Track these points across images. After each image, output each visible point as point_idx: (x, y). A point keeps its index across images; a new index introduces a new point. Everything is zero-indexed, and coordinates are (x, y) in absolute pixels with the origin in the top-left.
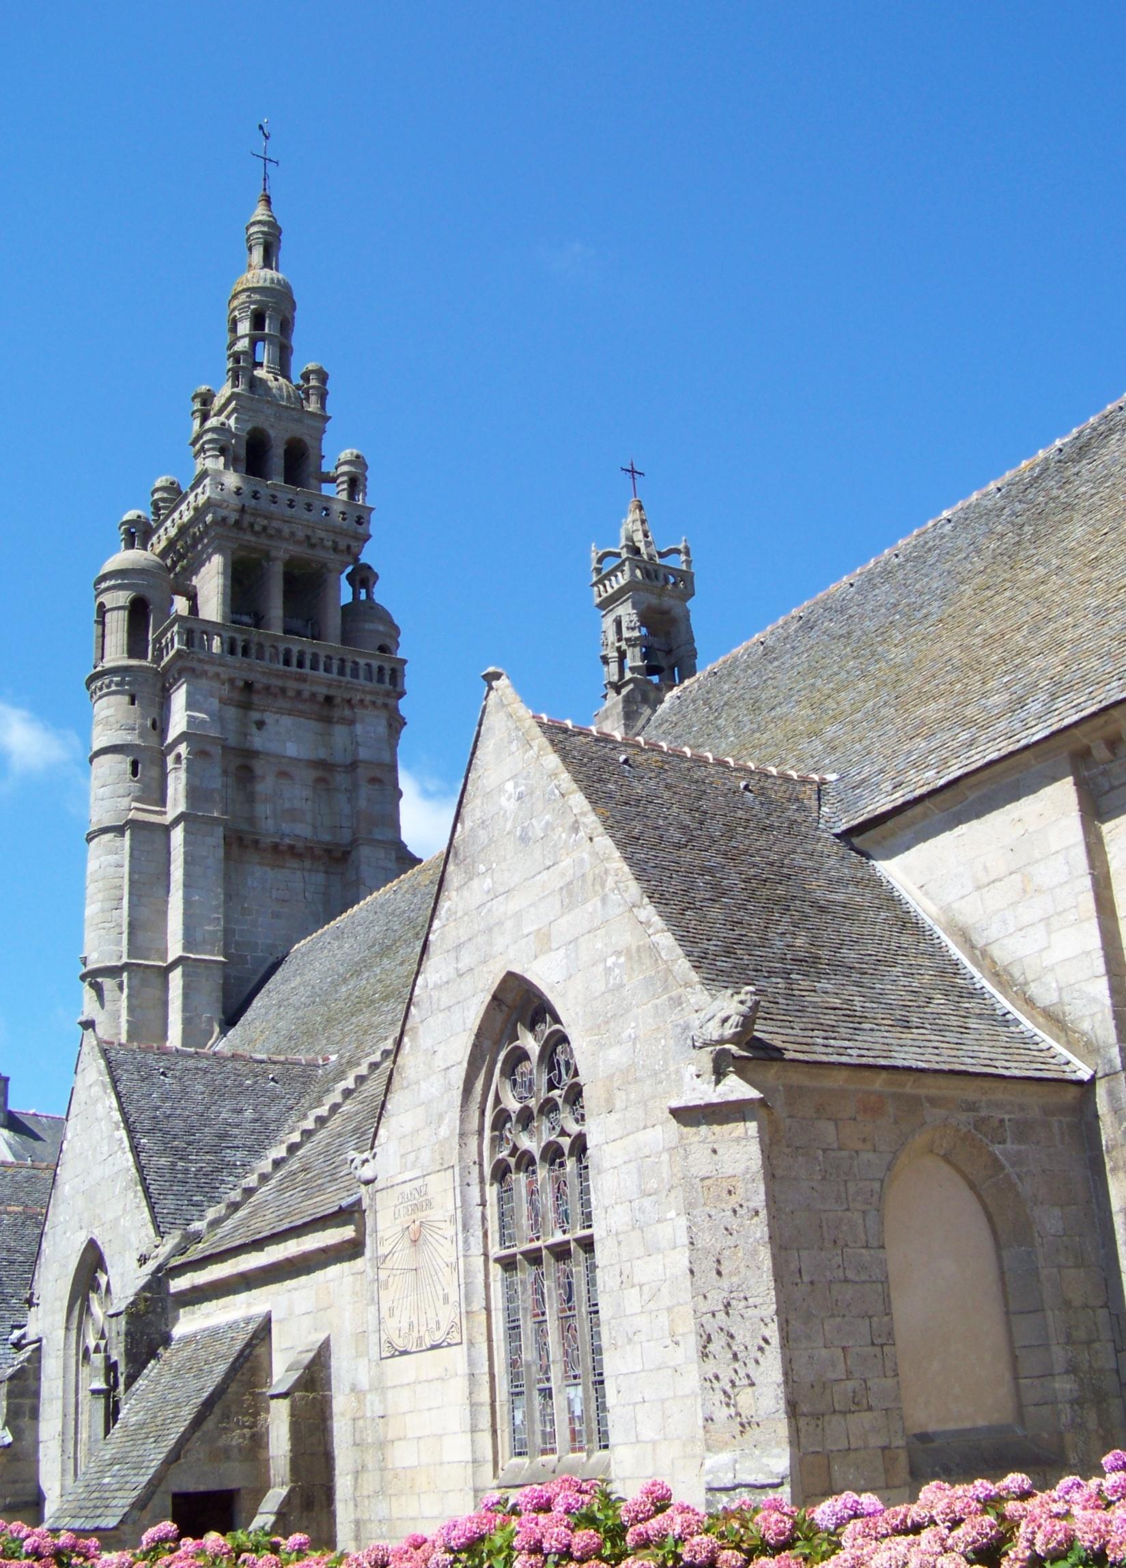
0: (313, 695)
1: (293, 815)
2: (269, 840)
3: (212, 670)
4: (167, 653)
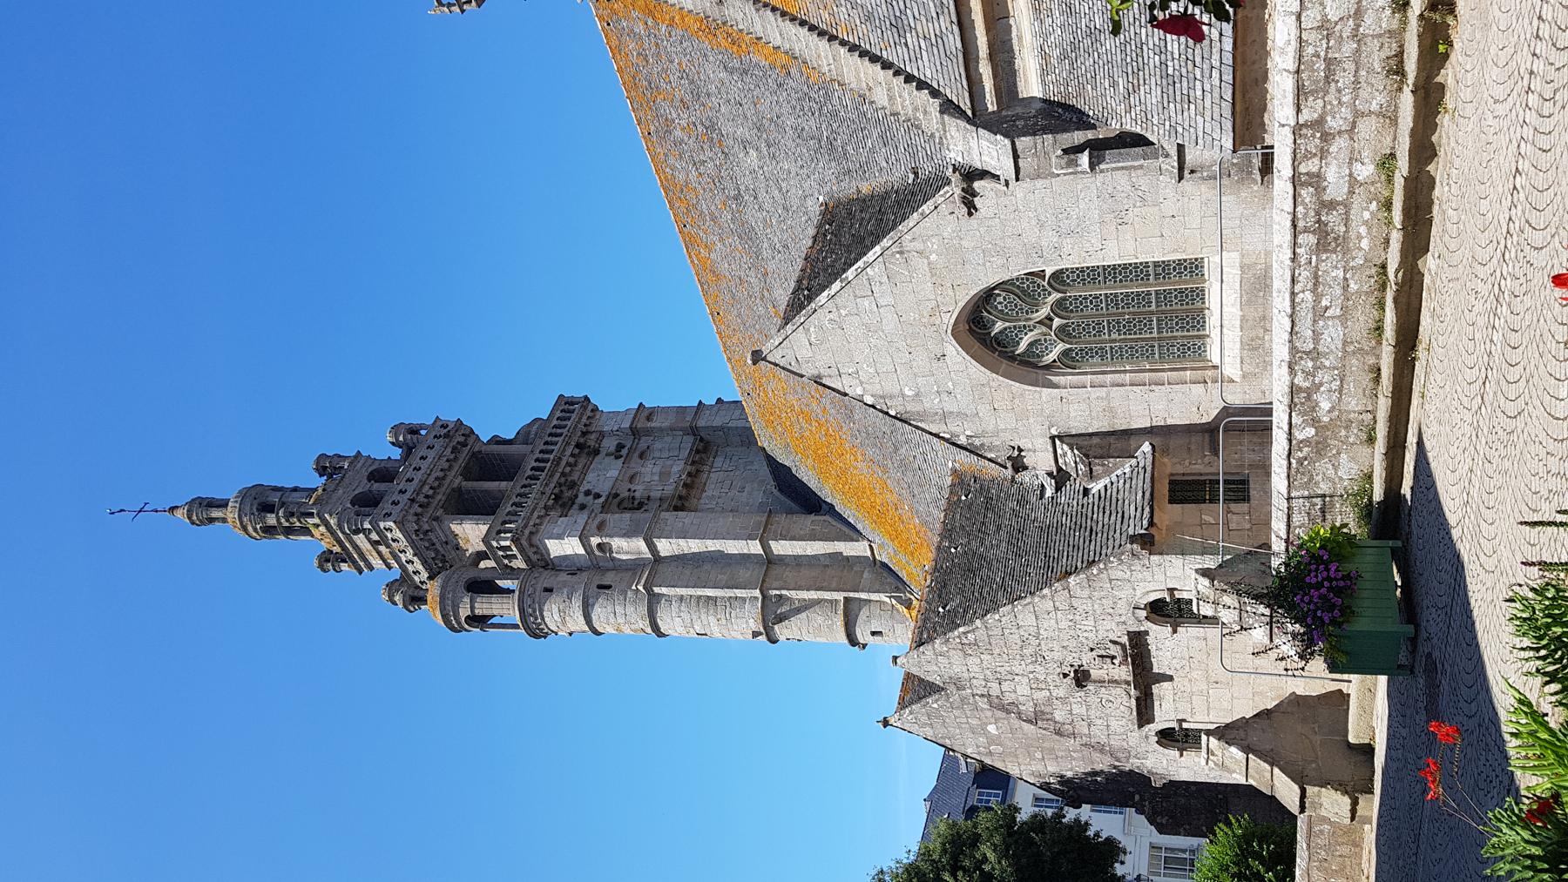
0: (572, 455)
1: (664, 475)
2: (681, 488)
4: (514, 557)
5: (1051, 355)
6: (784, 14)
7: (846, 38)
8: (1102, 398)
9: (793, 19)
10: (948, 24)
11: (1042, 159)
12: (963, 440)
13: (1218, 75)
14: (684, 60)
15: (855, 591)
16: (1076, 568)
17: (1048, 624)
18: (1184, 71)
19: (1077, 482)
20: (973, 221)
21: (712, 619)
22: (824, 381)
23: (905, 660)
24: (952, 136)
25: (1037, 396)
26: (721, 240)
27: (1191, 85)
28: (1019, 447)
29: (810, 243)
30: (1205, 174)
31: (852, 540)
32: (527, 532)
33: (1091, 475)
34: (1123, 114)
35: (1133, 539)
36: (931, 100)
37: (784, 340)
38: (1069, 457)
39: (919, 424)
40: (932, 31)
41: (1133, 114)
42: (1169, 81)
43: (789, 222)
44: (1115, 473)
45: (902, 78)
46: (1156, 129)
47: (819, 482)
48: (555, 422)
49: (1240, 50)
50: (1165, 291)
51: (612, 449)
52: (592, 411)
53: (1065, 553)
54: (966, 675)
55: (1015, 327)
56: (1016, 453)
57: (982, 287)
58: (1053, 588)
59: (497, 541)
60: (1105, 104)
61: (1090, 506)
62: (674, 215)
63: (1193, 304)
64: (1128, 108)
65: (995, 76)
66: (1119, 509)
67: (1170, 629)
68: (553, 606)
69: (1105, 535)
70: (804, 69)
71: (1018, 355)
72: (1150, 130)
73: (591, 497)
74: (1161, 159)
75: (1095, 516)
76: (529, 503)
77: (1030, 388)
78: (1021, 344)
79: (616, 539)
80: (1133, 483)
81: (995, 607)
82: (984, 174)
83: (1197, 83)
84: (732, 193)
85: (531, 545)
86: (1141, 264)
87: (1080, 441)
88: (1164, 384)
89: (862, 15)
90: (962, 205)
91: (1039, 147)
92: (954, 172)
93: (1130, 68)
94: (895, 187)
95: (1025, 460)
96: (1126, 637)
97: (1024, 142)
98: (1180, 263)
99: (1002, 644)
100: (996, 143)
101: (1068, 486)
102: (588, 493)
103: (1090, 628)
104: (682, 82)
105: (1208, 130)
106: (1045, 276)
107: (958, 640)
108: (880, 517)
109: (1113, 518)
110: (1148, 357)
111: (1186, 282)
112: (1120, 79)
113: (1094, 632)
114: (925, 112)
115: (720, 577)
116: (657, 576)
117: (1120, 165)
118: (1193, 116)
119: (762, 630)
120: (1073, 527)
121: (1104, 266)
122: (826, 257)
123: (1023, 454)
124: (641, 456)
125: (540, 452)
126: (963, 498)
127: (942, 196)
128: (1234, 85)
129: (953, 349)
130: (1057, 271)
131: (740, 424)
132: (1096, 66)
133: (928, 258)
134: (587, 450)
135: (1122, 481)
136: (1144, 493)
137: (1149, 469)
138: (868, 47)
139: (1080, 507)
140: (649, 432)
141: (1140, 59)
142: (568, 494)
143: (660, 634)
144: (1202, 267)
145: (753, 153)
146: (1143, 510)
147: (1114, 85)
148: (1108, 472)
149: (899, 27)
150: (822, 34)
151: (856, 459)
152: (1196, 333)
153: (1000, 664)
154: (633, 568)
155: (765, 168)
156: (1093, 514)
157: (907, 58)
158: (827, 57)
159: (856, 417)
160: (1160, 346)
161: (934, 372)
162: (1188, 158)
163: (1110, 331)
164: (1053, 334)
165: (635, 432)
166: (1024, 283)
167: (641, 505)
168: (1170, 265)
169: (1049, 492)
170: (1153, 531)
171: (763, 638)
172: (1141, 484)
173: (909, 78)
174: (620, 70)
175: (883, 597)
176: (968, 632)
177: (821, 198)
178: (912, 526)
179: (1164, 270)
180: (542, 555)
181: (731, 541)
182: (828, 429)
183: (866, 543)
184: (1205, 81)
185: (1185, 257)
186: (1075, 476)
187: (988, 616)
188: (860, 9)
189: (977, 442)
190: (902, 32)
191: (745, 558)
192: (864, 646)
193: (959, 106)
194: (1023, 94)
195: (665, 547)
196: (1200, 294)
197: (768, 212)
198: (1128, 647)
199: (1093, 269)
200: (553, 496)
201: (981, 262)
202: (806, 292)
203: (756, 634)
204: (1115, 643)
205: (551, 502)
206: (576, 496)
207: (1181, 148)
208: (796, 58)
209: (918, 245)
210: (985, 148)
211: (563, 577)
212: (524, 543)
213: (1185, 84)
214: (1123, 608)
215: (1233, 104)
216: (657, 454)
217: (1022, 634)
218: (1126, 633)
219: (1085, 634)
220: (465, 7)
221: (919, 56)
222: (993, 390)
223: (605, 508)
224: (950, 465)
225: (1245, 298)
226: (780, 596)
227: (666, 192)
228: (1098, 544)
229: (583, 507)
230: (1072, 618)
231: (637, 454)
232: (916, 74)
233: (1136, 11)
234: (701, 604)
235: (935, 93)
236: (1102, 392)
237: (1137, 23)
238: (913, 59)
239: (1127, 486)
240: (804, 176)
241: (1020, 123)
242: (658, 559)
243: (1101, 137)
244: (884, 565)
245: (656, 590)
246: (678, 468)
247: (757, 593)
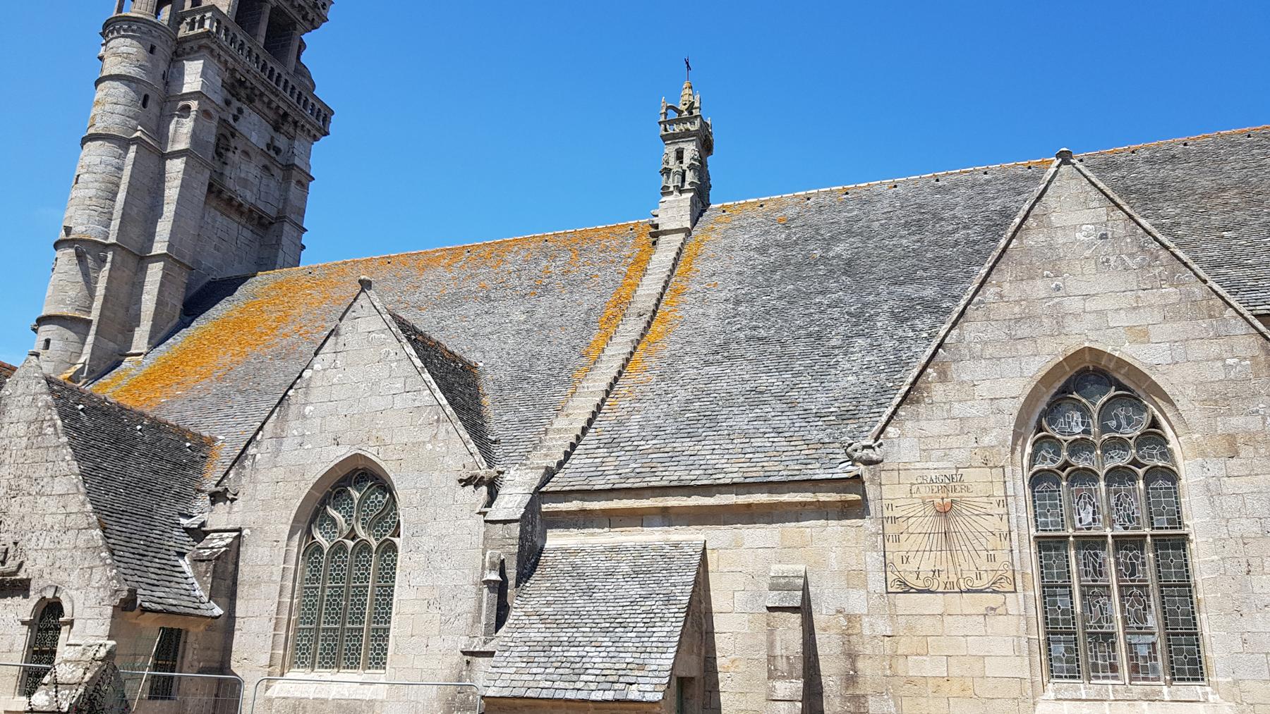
0: (278, 107)
1: (245, 183)
2: (229, 194)
3: (224, 56)
4: (192, 28)
5: (320, 536)
6: (628, 360)
7: (606, 403)
8: (270, 576)
9: (624, 366)
10: (612, 481)
11: (500, 543)
12: (252, 450)
13: (546, 686)
14: (599, 280)
15: (97, 332)
16: (108, 538)
17: (52, 505)
18: (553, 659)
19: (191, 548)
20: (454, 483)
21: (92, 192)
22: (332, 339)
23: (33, 364)
24: (527, 474)
25: (284, 521)
26: (454, 278)
27: (541, 665)
28: (236, 499)
29: (449, 348)
30: (464, 673)
31: (150, 338)
32: (214, 46)
33: (197, 561)
34: (524, 610)
35: (133, 593)
36: (556, 461)
37: (378, 311)
38: (218, 543)
39: (275, 414)
40: (607, 468)
41: (523, 618)
42: (547, 647)
43: (463, 336)
44: (196, 582)
45: (574, 441)
46: (510, 635)
47: (214, 318)
48: (311, 101)
49: (564, 704)
50: (362, 636)
51: (277, 144)
52: (315, 135)
53: (124, 529)
54: (7, 420)
55: (353, 508)
56: (230, 497)
57: (395, 484)
58: (91, 514)
59: (211, 18)
60: (533, 596)
61: (167, 557)
62: (478, 246)
63: (345, 659)
64: (528, 614)
65: (567, 512)
66: (161, 583)
67: (28, 618)
68: (135, 50)
69: (138, 567)
70: (584, 368)
71: (325, 508)
72: (510, 630)
73: (236, 113)
74: (484, 638)
75: (157, 560)
76: (241, 56)
77: (293, 515)
78: (335, 512)
79: (192, 124)
80: (185, 597)
81: (79, 457)
82: (492, 496)
83: (543, 669)
84: (492, 295)
85: (200, 47)
86: (390, 618)
87: (233, 554)
88: (275, 630)
89: (623, 418)
90: (469, 475)
91: (509, 541)
92: (498, 472)
93: (560, 617)
94: (485, 424)
95: (222, 503)
96: (25, 577)
97: (516, 529)
98: (384, 650)
99: (36, 460)
100: (518, 507)
101: (188, 539)
102: (240, 111)
103: (41, 544)
104: (583, 275)
105: (503, 677)
106: (394, 537)
107: (48, 417)
108: (169, 367)
109: (153, 576)
110: (302, 618)
111: (366, 654)
112: (552, 609)
113: (35, 547)
114: (546, 455)
115: (135, 209)
116: (147, 152)
117: (485, 605)
118: (517, 665)
119: (71, 237)
120: (148, 539)
121: (393, 587)
122: (438, 359)
123: (228, 502)
124: (265, 167)
125: (286, 80)
126: (188, 444)
127: (480, 460)
128: (538, 698)
129: (343, 452)
130: (396, 547)
131: (280, 260)
132: (564, 591)
133: (429, 442)
134: (280, 121)
135: (188, 587)
136: (175, 605)
137: (197, 612)
138: (598, 419)
139: (167, 548)
140: (287, 179)
141: (566, 626)
142: (243, 93)
143: (85, 140)
144: (377, 668)
145: (523, 317)
146: (159, 603)
147: (548, 604)
148: (198, 576)
149: (612, 444)
150: (611, 386)
151: (233, 355)
152: (317, 661)
153: (14, 455)
154: (160, 133)
155: (510, 325)
156: (159, 559)
157: (588, 447)
158: (594, 386)
159: (277, 362)
160: (310, 629)
161: (323, 435)
162: (481, 660)
163: (333, 588)
164: (340, 539)
165: (289, 167)
166: (391, 519)
167: (219, 155)
168: (383, 641)
169: (184, 522)
170: (137, 611)
171: (62, 235)
172: (184, 604)
173: (573, 446)
174: (598, 230)
175: (85, 357)
176: (55, 428)
177: (481, 364)
178: (158, 395)
179: (381, 636)
180: (188, 54)
181: (170, 227)
182: (267, 335)
183: (145, 350)
184: (544, 676)
185: (389, 654)
186: (199, 546)
187: (70, 450)
188: (627, 417)
189: (247, 463)
190: (607, 446)
191: (150, 237)
192: (35, 330)
193: (549, 482)
194: (550, 533)
195: (175, 168)
196: (353, 664)
197: (474, 320)
198: (13, 578)
199: (392, 578)
200: (243, 79)
201: (418, 485)
202: (413, 337)
203: (68, 230)
204: (20, 565)
205: (238, 76)
206: (239, 100)
207: (491, 654)
208: (595, 364)
209: (442, 435)
210: (516, 498)
211: (163, 67)
212: (204, 41)
213: (543, 660)
214: (59, 576)
215: (523, 698)
216: (264, 181)
217: (45, 480)
218: (30, 577)
219: (34, 539)
220: (663, 126)
221: (589, 456)
222: (297, 483)
223: (223, 122)
224: (220, 437)
225: (344, 702)
226: (104, 261)
227: (498, 243)
228: (130, 560)
229: (228, 103)
230: (55, 528)
231: (268, 163)
232: (575, 452)
233: (603, 625)
234: (111, 185)
235: (560, 465)
236: (277, 577)
237: (594, 625)
238: (587, 452)
239: (183, 592)
240: (501, 354)
241: (529, 528)
242: (165, 157)
243: (509, 591)
244: (119, 363)
245: (133, 148)
246: (248, 196)
247: (112, 240)
